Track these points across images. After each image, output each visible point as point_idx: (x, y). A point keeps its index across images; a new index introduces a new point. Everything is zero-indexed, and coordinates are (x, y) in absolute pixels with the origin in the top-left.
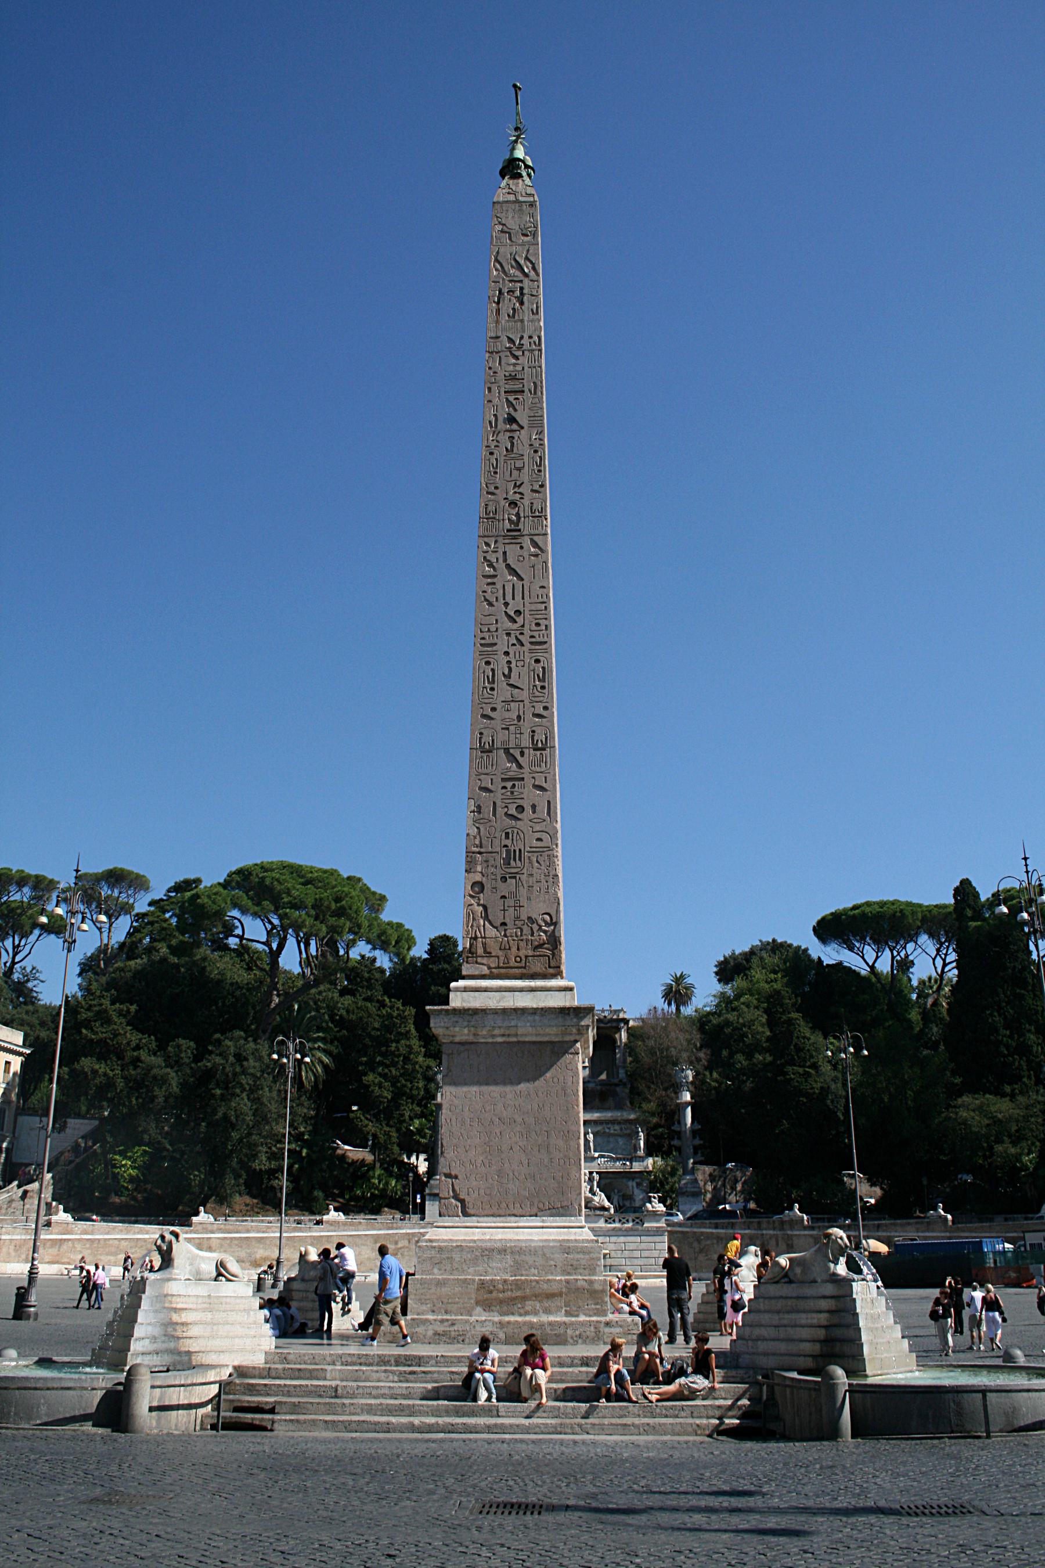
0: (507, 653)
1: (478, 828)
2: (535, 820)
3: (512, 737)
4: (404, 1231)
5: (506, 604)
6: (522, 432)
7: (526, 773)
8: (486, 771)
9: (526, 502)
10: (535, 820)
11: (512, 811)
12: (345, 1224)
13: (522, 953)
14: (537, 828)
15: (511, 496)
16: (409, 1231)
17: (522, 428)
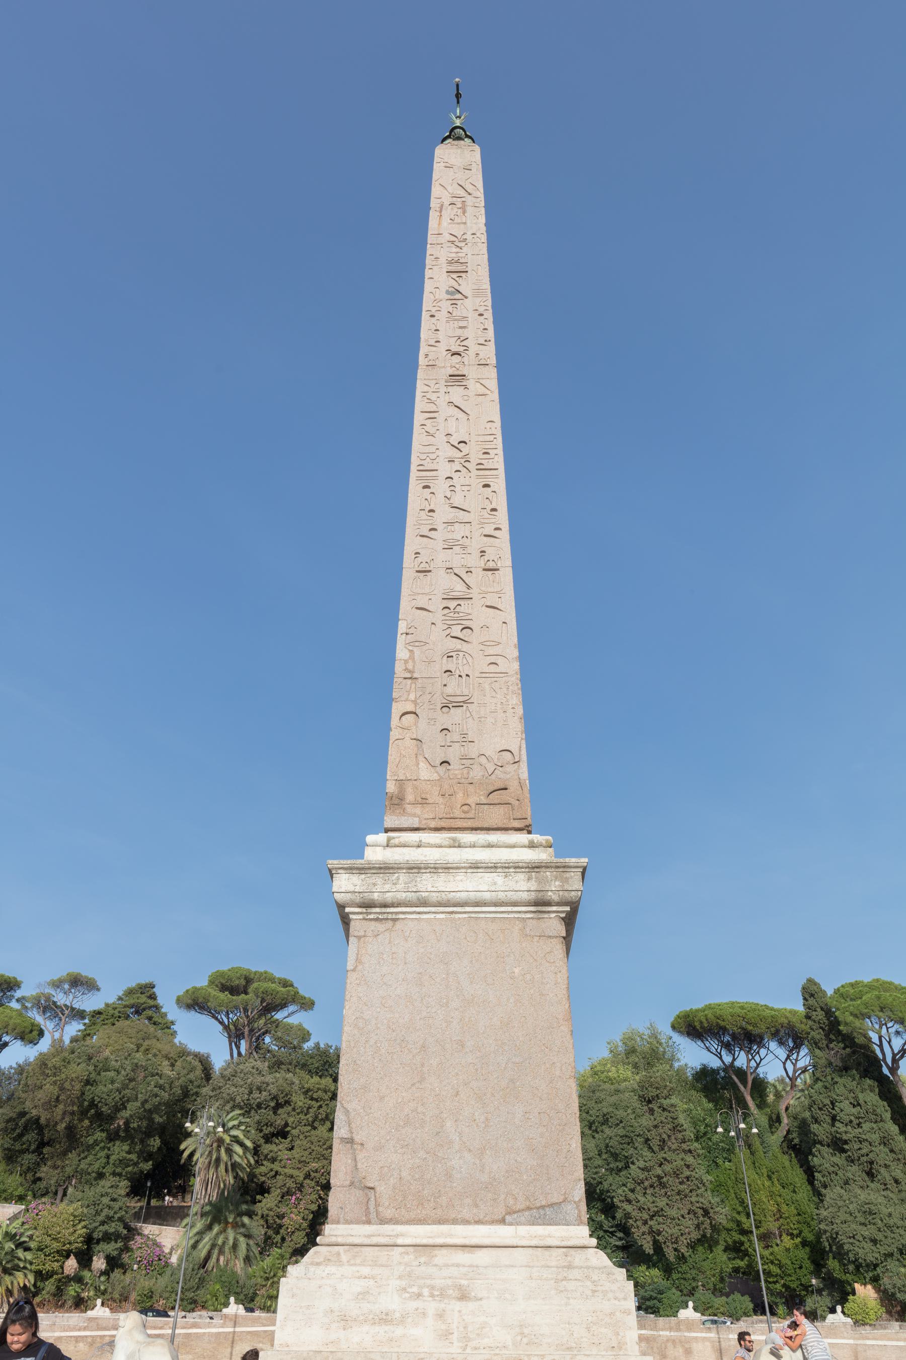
1: (411, 651)
2: (488, 643)
7: (474, 593)
8: (423, 591)
9: (471, 352)
10: (488, 643)
14: (491, 651)
17: (466, 298)
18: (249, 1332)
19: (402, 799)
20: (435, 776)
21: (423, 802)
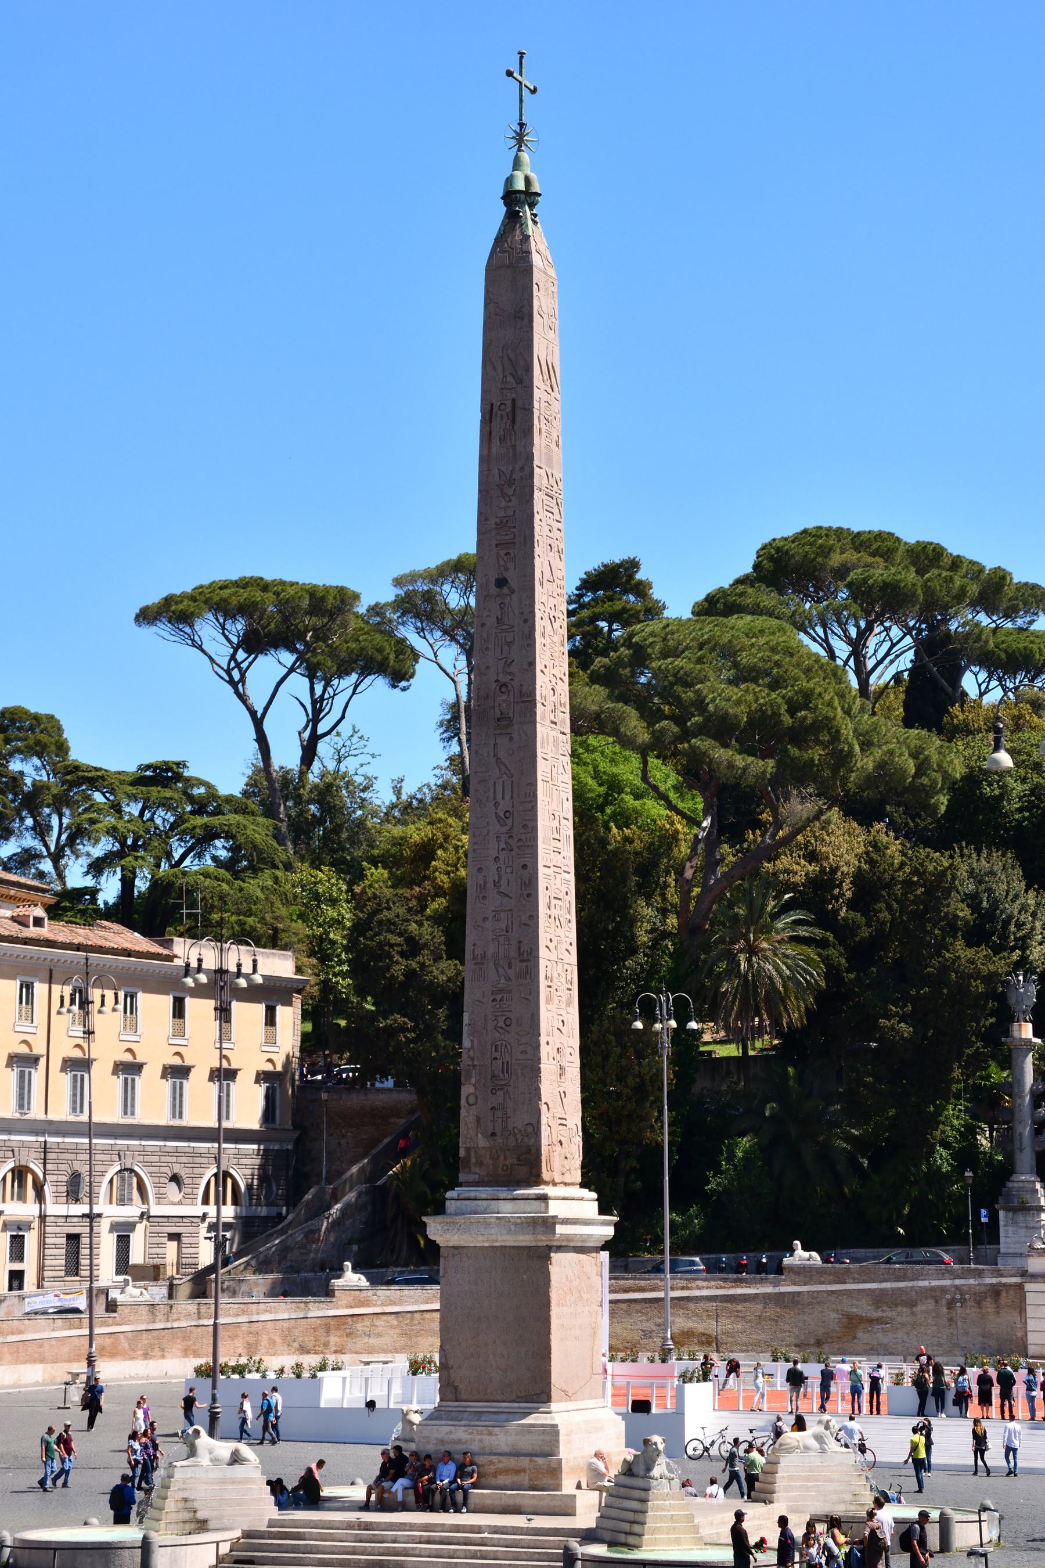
1: (472, 1041)
3: (502, 948)
4: (926, 1283)
5: (496, 805)
6: (514, 596)
11: (501, 1024)
12: (820, 1271)
13: (508, 1162)
15: (502, 679)
16: (935, 1283)
18: (833, 1292)
19: (469, 1161)
20: (488, 1145)
21: (480, 1164)
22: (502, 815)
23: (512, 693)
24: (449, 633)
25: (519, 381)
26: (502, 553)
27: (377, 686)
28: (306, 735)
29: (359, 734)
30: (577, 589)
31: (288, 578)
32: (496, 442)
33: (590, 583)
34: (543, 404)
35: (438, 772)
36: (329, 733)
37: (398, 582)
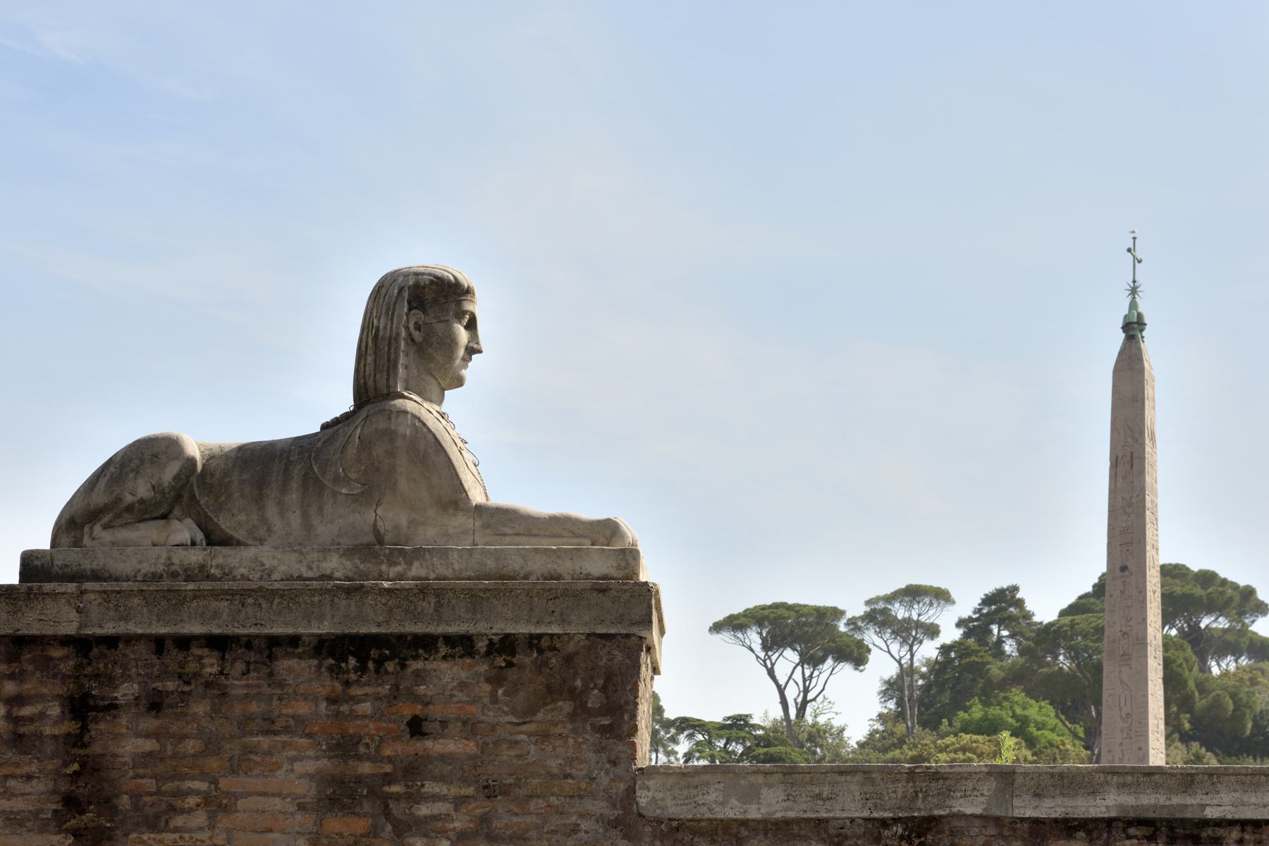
0: (1121, 744)
5: (1121, 709)
15: (1125, 630)
22: (1124, 716)
23: (1131, 639)
24: (896, 633)
25: (1136, 441)
26: (1125, 550)
27: (846, 669)
28: (799, 700)
29: (828, 700)
30: (979, 605)
31: (802, 602)
32: (1120, 480)
33: (988, 600)
34: (1150, 455)
35: (871, 722)
36: (814, 699)
37: (868, 603)
